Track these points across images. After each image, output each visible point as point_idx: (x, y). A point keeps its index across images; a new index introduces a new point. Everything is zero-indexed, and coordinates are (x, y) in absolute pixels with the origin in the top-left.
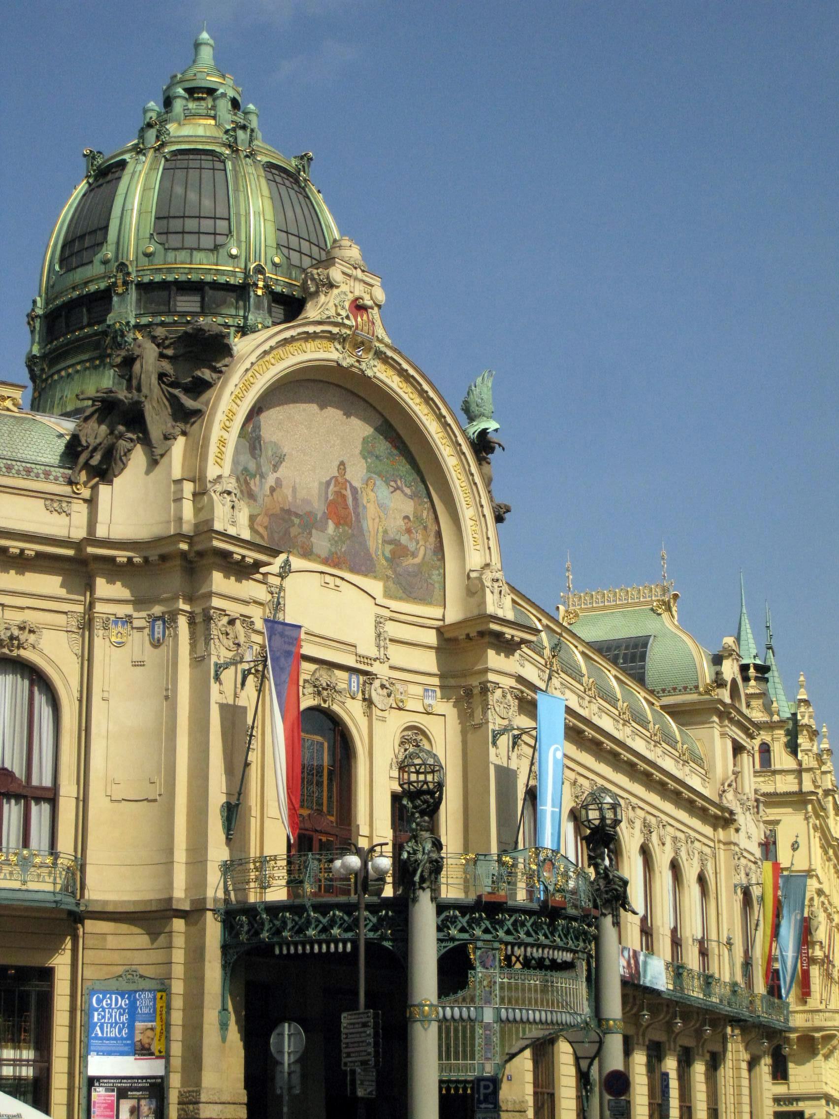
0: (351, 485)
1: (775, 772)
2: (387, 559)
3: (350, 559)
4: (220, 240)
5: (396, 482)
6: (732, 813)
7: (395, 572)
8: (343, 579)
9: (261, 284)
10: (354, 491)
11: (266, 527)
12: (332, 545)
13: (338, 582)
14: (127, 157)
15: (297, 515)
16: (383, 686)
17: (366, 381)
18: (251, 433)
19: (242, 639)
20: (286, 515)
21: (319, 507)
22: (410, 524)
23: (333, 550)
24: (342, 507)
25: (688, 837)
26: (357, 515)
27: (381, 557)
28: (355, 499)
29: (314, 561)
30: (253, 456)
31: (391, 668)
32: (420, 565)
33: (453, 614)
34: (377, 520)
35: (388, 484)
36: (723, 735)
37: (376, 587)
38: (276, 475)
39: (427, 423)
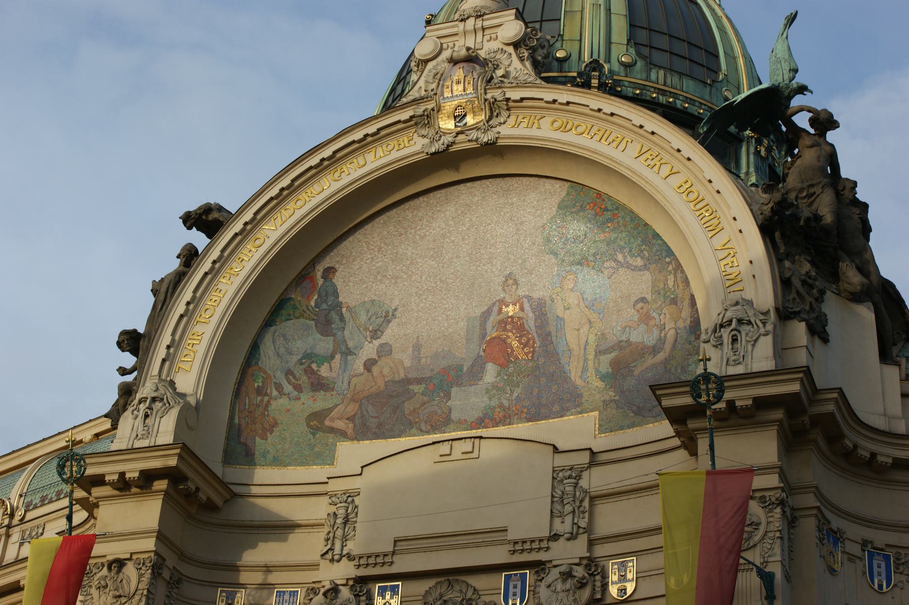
0: (529, 298)
2: (603, 378)
8: (481, 438)
11: (351, 419)
12: (490, 399)
13: (467, 446)
15: (419, 381)
17: (492, 150)
18: (316, 306)
22: (645, 310)
23: (494, 402)
26: (546, 337)
29: (454, 431)
32: (666, 362)
34: (586, 328)
38: (376, 343)
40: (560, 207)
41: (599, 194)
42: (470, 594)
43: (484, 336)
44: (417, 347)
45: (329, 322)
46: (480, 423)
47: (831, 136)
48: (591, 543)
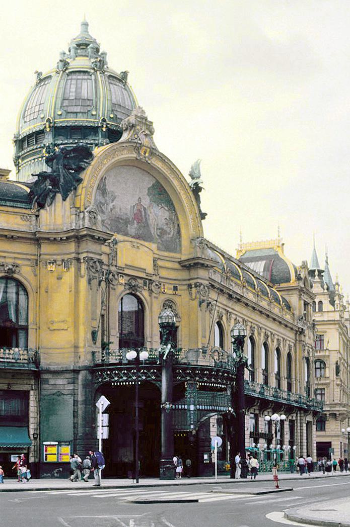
1: (324, 312)
2: (158, 236)
3: (144, 236)
4: (89, 108)
5: (161, 205)
6: (302, 329)
7: (162, 241)
9: (105, 126)
10: (145, 209)
14: (52, 74)
15: (121, 219)
16: (156, 285)
19: (99, 269)
20: (117, 219)
21: (130, 216)
24: (140, 216)
25: (284, 339)
27: (156, 235)
28: (145, 212)
30: (104, 197)
31: (160, 277)
32: (172, 237)
33: (184, 258)
34: (154, 220)
35: (158, 206)
36: (300, 298)
37: (154, 246)
39: (173, 181)
40: (153, 185)
41: (161, 185)
42: (137, 283)
43: (134, 212)
44: (120, 209)
45: (104, 194)
46: (133, 237)
47: (199, 193)
48: (160, 277)
